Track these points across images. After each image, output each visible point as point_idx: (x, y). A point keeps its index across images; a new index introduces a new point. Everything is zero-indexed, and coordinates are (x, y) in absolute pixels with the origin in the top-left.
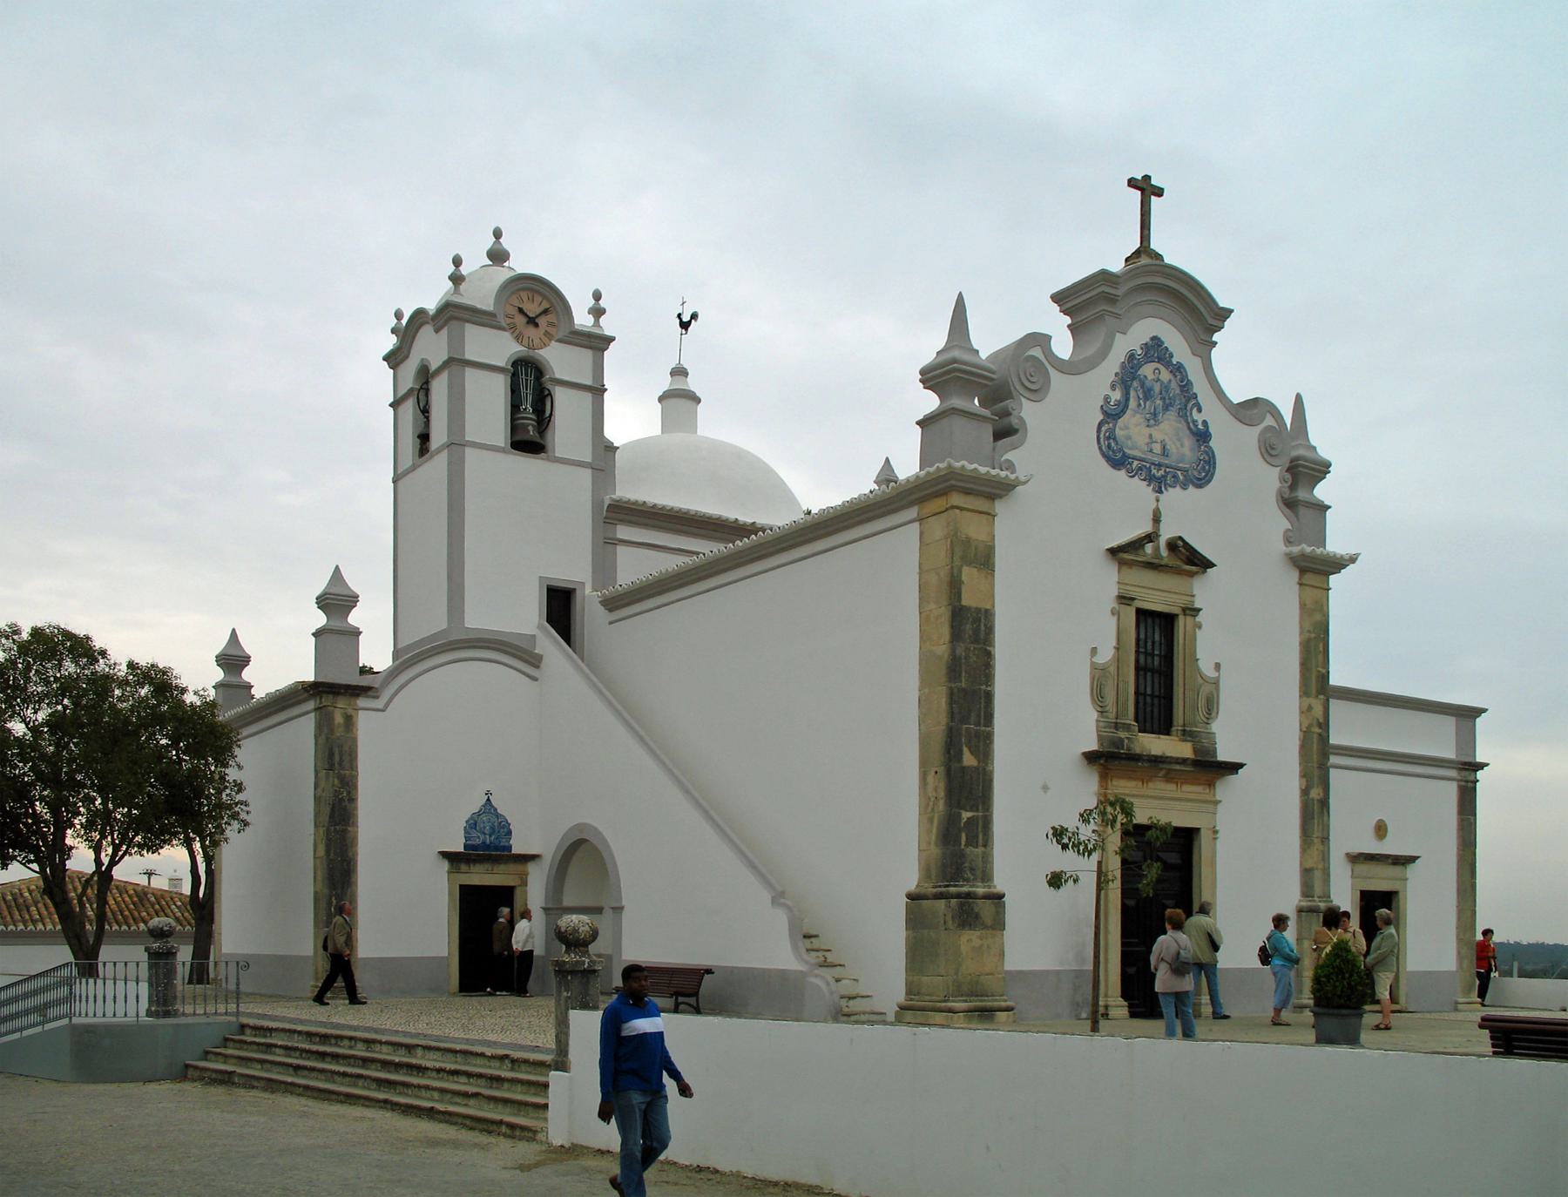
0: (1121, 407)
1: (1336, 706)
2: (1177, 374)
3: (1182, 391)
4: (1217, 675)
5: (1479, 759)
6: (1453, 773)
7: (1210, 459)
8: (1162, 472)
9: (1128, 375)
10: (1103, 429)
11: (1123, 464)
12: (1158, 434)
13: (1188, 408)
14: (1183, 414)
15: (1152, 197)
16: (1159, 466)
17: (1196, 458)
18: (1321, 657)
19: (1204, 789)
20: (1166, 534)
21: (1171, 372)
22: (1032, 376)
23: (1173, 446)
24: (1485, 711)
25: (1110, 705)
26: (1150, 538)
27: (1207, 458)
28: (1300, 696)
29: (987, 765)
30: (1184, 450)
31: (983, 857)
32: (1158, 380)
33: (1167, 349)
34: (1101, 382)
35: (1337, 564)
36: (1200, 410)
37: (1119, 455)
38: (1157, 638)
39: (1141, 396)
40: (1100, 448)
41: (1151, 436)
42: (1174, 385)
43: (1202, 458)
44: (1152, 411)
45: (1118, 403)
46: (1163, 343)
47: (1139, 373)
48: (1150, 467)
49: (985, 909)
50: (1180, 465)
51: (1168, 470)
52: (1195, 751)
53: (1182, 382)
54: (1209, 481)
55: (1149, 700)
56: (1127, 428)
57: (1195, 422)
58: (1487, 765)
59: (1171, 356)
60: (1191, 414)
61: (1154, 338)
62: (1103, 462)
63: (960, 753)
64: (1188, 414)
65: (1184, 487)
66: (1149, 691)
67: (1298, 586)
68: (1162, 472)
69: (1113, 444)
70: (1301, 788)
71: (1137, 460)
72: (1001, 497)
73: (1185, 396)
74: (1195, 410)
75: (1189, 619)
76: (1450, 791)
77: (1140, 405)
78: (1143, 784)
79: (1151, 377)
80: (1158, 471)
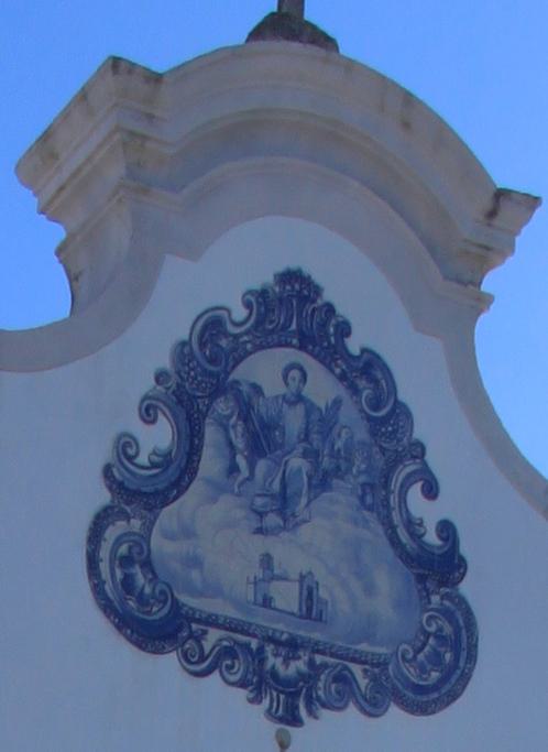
12: (291, 555)
16: (292, 646)
37: (158, 613)
40: (98, 589)
41: (267, 561)
45: (163, 461)
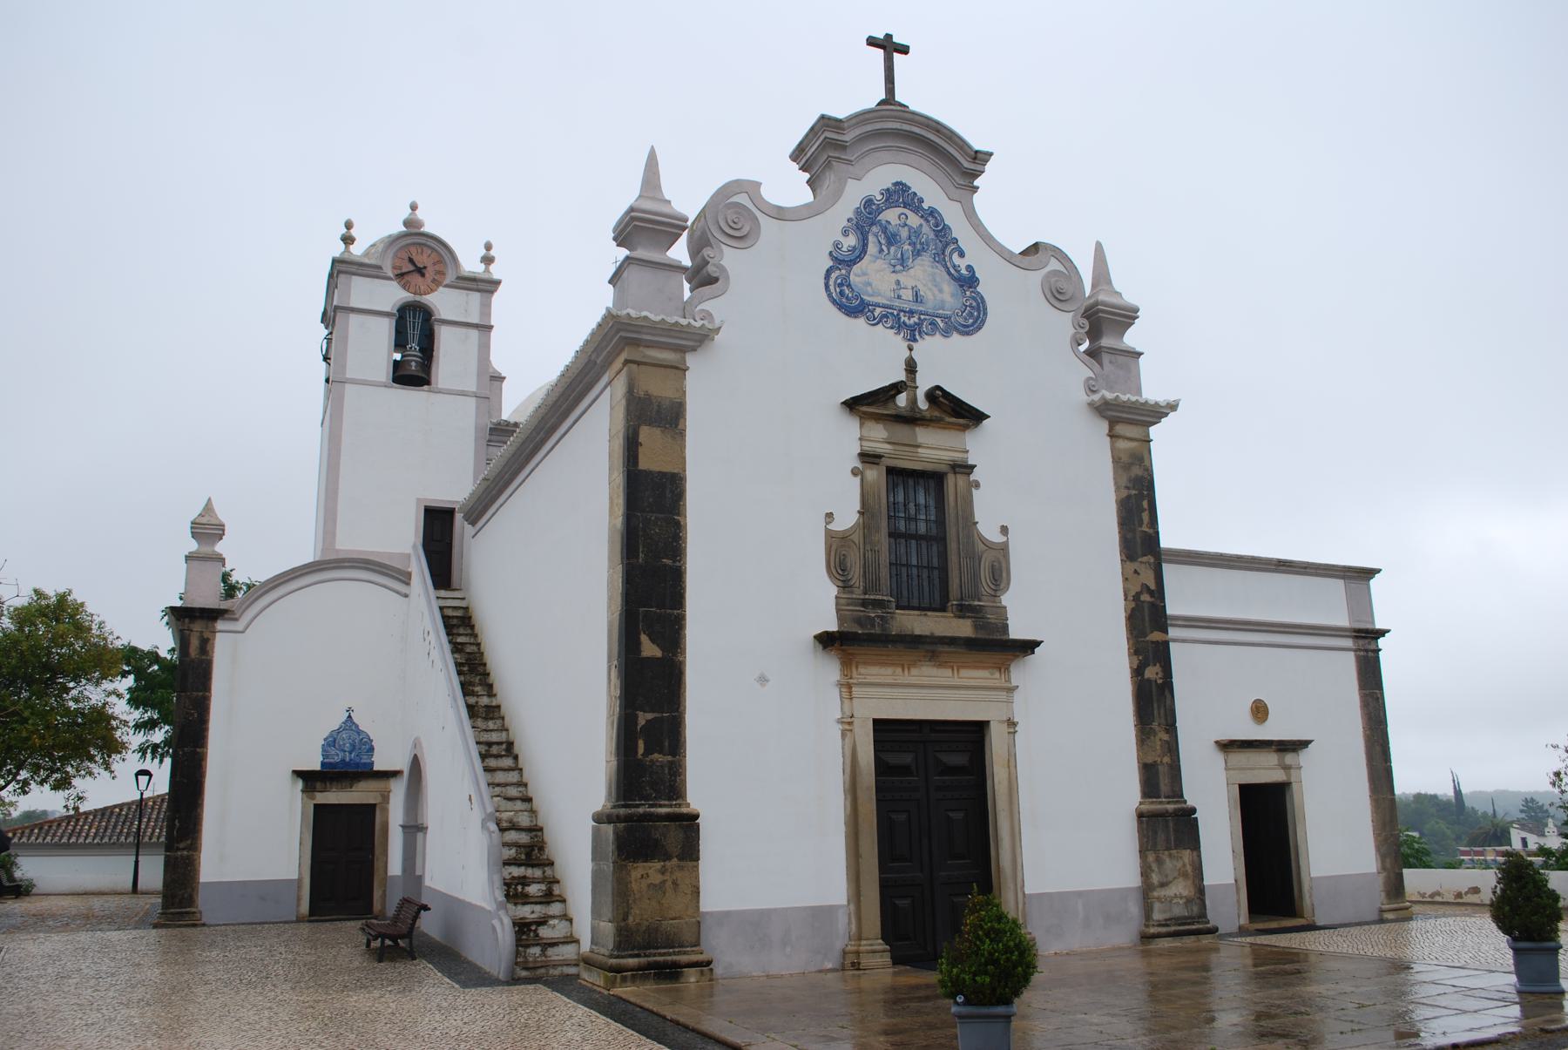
0: (857, 253)
1: (1168, 570)
2: (930, 219)
3: (937, 236)
4: (1004, 539)
5: (1379, 625)
6: (1349, 643)
7: (978, 305)
8: (915, 319)
9: (866, 219)
10: (834, 276)
11: (861, 312)
12: (907, 279)
13: (947, 252)
14: (940, 258)
15: (895, 54)
16: (911, 313)
17: (960, 305)
18: (1146, 516)
19: (992, 674)
20: (924, 383)
21: (922, 217)
22: (735, 223)
24: (1378, 571)
25: (856, 576)
26: (896, 388)
27: (974, 304)
28: (1122, 560)
29: (675, 655)
30: (944, 296)
31: (670, 769)
33: (915, 194)
34: (833, 226)
35: (1157, 413)
36: (962, 255)
37: (856, 303)
38: (921, 500)
39: (883, 242)
40: (830, 296)
41: (898, 282)
42: (926, 229)
44: (899, 256)
46: (909, 188)
47: (878, 218)
49: (673, 837)
50: (941, 312)
51: (922, 317)
52: (976, 627)
54: (979, 328)
55: (915, 571)
56: (864, 274)
58: (1388, 631)
59: (921, 201)
60: (951, 258)
62: (834, 310)
63: (638, 644)
64: (947, 259)
65: (946, 333)
66: (914, 562)
67: (1108, 438)
68: (915, 319)
69: (847, 292)
70: (1131, 667)
72: (694, 349)
73: (941, 241)
74: (955, 256)
75: (961, 480)
76: (1346, 665)
78: (903, 670)
79: (894, 221)
80: (909, 319)
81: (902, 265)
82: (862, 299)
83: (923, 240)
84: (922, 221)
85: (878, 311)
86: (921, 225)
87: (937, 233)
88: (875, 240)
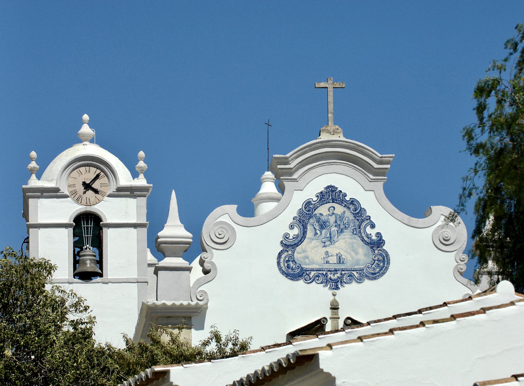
0: (299, 239)
2: (351, 206)
3: (355, 217)
7: (384, 259)
10: (283, 256)
12: (333, 250)
13: (362, 227)
14: (358, 231)
22: (220, 235)
23: (349, 257)
32: (333, 214)
33: (341, 191)
36: (373, 226)
39: (317, 228)
40: (280, 269)
41: (327, 253)
43: (376, 259)
44: (328, 235)
46: (337, 188)
48: (326, 274)
50: (356, 267)
51: (343, 272)
53: (356, 211)
56: (304, 251)
57: (368, 236)
60: (365, 231)
61: (329, 187)
64: (362, 231)
65: (360, 281)
71: (314, 271)
77: (316, 234)
80: (334, 275)
81: (330, 241)
82: (302, 268)
83: (345, 221)
84: (345, 209)
85: (313, 273)
86: (344, 212)
87: (356, 215)
88: (312, 228)
